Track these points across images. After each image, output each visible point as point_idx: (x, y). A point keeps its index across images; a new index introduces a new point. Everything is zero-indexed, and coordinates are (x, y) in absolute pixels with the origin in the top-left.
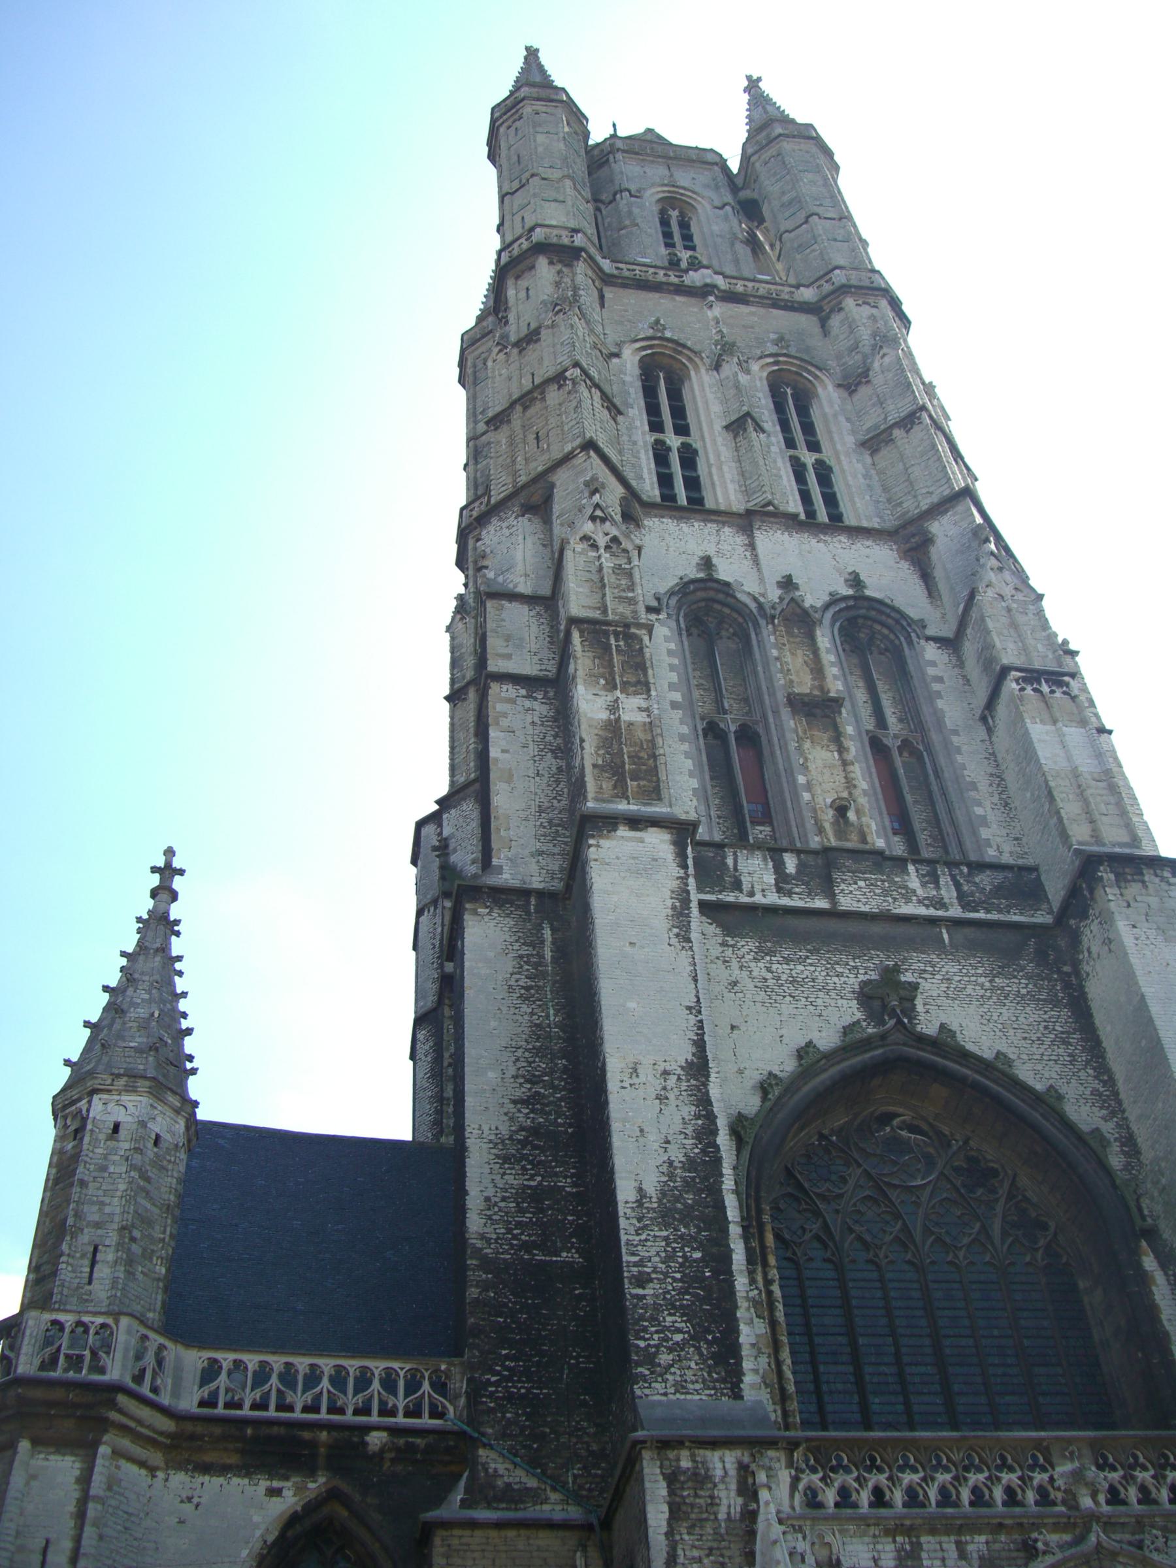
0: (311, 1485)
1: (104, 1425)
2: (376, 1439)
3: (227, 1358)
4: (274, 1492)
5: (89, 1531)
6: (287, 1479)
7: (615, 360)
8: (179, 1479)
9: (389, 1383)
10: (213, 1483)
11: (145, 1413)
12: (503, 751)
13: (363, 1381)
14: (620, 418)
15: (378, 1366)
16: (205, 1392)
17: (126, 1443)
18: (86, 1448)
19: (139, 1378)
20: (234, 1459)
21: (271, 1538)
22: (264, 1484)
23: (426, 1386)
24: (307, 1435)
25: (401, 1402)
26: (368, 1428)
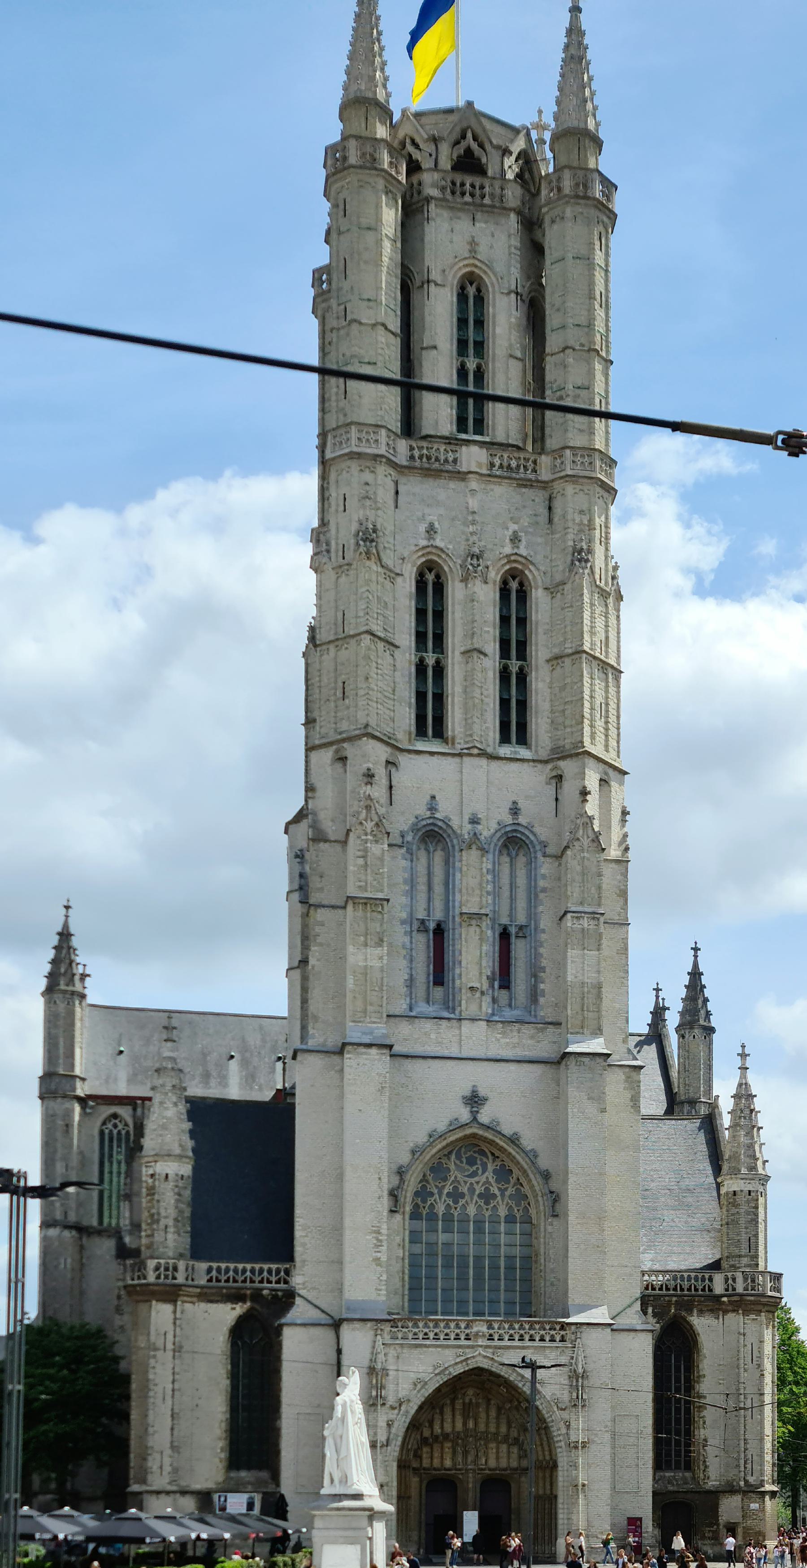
0: (245, 1306)
1: (179, 1295)
2: (265, 1292)
3: (215, 1265)
4: (234, 1309)
5: (178, 1330)
6: (237, 1304)
7: (399, 580)
8: (203, 1306)
9: (270, 1271)
10: (214, 1308)
11: (191, 1289)
12: (318, 960)
13: (261, 1271)
14: (397, 653)
15: (266, 1267)
16: (208, 1277)
17: (185, 1299)
18: (174, 1302)
19: (187, 1279)
20: (219, 1298)
21: (233, 1324)
22: (229, 1306)
23: (282, 1273)
24: (242, 1292)
25: (274, 1279)
26: (262, 1289)
